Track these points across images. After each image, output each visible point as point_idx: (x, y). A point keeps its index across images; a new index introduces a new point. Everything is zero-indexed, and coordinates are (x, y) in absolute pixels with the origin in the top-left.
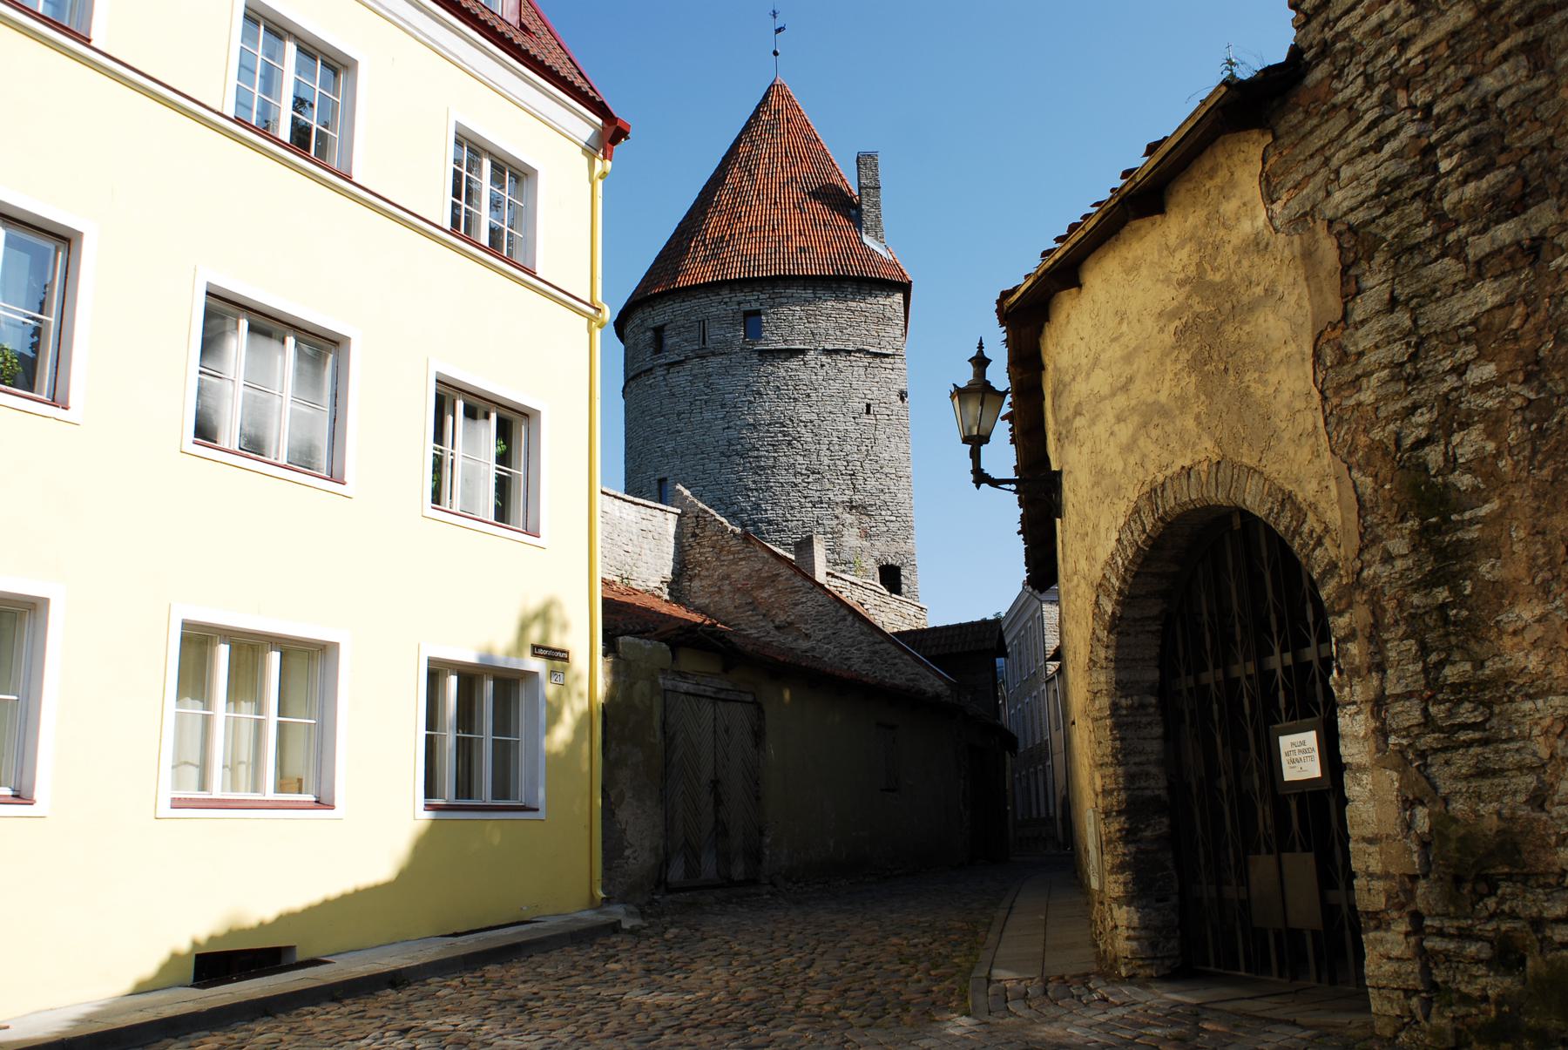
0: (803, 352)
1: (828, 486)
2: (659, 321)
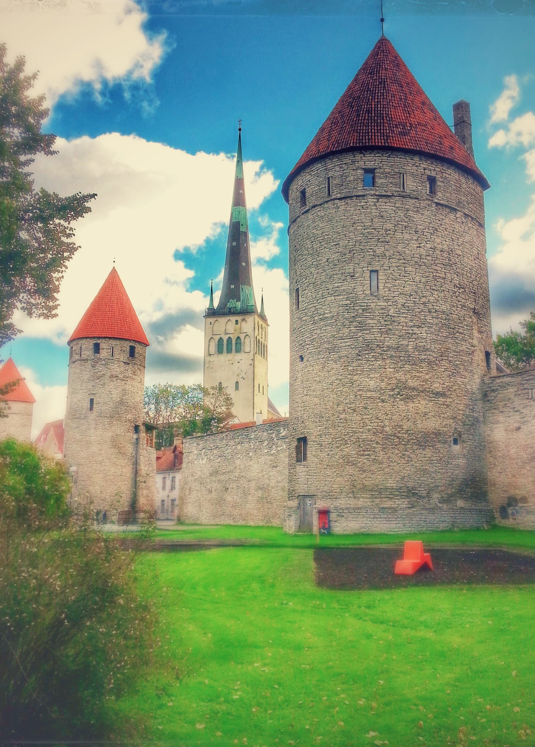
0: (455, 210)
2: (370, 165)
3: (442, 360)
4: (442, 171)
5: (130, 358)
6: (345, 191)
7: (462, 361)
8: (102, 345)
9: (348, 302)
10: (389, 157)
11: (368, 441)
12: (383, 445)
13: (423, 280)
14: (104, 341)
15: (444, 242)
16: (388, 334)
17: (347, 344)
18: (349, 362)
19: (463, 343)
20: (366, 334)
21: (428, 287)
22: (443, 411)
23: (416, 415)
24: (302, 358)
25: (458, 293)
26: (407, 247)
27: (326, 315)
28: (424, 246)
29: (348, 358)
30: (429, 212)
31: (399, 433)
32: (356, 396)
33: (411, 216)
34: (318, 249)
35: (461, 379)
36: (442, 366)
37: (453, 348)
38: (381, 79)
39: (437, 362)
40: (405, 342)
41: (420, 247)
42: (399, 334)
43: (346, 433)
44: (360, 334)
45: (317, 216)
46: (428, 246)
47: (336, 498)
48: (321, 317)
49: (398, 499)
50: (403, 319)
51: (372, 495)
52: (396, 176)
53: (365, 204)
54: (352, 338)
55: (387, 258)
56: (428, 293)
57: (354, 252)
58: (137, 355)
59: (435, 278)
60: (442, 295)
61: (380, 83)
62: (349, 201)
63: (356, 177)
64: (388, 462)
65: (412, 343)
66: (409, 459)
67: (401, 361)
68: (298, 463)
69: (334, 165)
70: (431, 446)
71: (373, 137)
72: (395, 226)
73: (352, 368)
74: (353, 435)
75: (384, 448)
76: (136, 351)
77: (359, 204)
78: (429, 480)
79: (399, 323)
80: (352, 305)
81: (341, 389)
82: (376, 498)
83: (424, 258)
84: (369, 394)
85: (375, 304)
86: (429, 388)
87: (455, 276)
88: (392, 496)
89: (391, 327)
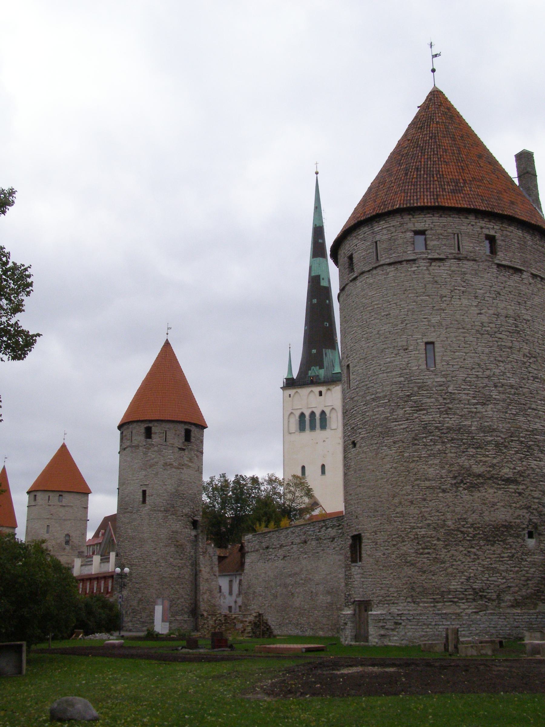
1: (540, 368)
2: (419, 226)
3: (512, 441)
4: (502, 229)
5: (186, 443)
6: (394, 255)
7: (535, 442)
8: (154, 430)
9: (402, 379)
10: (441, 217)
11: (428, 537)
12: (444, 541)
13: (487, 350)
14: (156, 424)
15: (509, 307)
16: (447, 414)
17: (402, 427)
18: (404, 447)
19: (537, 420)
20: (423, 415)
21: (492, 359)
22: (515, 499)
23: (483, 506)
24: (354, 444)
25: (528, 364)
26: (466, 315)
27: (378, 395)
28: (485, 312)
29: (403, 442)
30: (489, 274)
31: (463, 527)
32: (413, 487)
33: (468, 280)
34: (368, 320)
35: (535, 462)
36: (511, 447)
37: (525, 426)
38: (432, 133)
39: (506, 444)
40: (468, 423)
41: (481, 314)
42: (460, 414)
43: (403, 529)
44: (416, 415)
45: (366, 283)
46: (491, 312)
47: (393, 603)
48: (373, 396)
49: (463, 603)
50: (464, 397)
51: (434, 599)
52: (449, 237)
53: (416, 268)
54: (407, 420)
55: (444, 328)
56: (492, 365)
57: (407, 322)
58: (193, 440)
59: (500, 348)
60: (509, 366)
61: (431, 138)
62: (399, 266)
63: (405, 240)
64: (452, 561)
65: (476, 423)
66: (475, 557)
67: (464, 444)
68: (353, 564)
69: (381, 228)
70: (501, 541)
71: (422, 197)
72: (452, 291)
73: (408, 454)
74: (410, 532)
75: (446, 545)
76: (192, 434)
77: (409, 269)
78: (500, 580)
79: (460, 401)
80: (407, 382)
81: (397, 478)
82: (437, 602)
83: (487, 325)
84: (428, 483)
85: (432, 380)
86: (497, 474)
87: (524, 344)
88: (456, 600)
89: (450, 406)
